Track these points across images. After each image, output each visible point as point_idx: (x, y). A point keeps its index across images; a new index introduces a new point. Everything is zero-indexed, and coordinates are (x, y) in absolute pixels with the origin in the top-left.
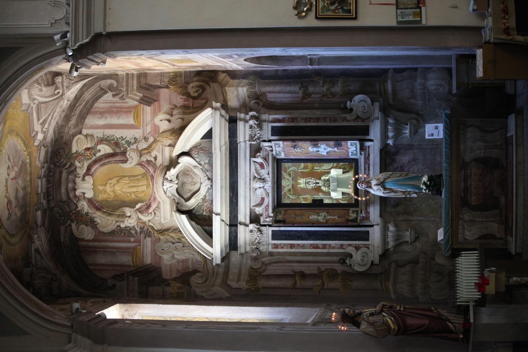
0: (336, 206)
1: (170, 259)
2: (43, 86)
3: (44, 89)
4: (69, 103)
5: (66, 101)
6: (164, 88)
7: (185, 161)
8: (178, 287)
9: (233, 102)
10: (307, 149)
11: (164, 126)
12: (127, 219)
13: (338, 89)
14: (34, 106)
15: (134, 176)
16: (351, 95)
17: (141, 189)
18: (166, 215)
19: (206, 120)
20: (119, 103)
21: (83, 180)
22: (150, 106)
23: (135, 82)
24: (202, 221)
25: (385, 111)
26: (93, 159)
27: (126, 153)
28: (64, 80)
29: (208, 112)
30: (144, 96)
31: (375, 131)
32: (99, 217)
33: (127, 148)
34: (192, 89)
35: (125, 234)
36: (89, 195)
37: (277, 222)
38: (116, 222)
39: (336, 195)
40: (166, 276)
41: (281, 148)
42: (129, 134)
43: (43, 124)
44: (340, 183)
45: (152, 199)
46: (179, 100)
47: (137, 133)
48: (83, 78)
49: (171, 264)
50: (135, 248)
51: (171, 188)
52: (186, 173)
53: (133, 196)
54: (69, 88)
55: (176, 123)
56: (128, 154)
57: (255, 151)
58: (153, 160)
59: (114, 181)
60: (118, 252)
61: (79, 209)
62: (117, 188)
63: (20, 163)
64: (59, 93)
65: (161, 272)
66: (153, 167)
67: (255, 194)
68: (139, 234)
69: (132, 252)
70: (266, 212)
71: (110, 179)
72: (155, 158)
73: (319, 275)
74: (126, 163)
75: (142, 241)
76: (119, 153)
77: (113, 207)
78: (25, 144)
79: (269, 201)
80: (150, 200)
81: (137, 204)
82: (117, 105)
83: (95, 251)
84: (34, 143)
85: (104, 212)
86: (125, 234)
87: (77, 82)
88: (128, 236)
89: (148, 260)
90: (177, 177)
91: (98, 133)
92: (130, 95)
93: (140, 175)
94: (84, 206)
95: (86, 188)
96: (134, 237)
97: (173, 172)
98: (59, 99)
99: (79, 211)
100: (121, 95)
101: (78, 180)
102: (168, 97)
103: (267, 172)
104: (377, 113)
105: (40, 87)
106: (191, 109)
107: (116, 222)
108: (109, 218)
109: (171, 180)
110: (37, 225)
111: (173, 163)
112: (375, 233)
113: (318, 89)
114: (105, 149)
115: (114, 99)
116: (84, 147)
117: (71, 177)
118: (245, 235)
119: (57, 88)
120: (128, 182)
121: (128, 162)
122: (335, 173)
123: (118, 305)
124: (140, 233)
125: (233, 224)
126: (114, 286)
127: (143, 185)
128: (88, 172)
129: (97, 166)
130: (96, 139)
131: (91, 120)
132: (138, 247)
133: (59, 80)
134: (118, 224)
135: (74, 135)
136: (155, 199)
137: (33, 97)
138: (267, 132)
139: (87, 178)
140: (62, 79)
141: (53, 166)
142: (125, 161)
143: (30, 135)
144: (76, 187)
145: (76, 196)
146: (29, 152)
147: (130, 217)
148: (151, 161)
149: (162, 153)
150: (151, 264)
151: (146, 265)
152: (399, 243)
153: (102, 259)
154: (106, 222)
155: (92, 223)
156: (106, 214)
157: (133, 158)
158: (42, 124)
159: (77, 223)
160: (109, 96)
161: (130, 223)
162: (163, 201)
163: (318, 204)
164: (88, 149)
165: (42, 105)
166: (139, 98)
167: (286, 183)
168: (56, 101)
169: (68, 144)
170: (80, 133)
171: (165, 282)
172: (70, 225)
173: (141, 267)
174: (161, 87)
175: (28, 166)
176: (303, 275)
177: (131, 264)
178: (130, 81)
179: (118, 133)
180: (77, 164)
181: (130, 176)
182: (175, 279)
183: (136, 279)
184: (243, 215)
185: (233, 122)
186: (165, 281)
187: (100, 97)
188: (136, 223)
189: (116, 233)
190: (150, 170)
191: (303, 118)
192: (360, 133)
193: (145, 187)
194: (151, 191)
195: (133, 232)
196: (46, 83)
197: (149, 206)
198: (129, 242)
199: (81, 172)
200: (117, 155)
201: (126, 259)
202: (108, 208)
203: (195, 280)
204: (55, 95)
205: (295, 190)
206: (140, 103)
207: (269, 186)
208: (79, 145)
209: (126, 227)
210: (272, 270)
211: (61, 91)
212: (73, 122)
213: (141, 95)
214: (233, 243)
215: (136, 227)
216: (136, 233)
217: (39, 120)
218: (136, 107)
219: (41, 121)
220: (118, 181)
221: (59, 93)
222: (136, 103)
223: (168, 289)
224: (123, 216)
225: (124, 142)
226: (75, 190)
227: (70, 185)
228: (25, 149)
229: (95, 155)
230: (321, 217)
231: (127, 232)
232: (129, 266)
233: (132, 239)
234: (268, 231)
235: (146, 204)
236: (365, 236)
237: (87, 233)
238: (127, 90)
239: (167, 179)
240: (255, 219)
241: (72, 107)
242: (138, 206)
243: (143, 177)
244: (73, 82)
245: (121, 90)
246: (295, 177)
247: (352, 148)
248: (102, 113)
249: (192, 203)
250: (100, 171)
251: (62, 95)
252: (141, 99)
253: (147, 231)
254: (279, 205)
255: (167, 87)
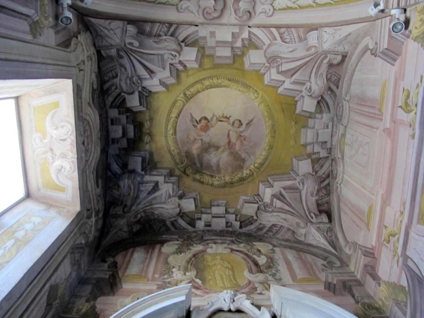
2: (317, 198)
3: (314, 199)
4: (302, 239)
5: (303, 231)
6: (355, 300)
8: (82, 309)
12: (183, 273)
14: (296, 182)
15: (235, 278)
20: (318, 268)
21: (226, 248)
22: (325, 288)
23: (348, 278)
26: (249, 254)
27: (261, 273)
28: (326, 225)
30: (335, 285)
33: (267, 273)
35: (164, 271)
36: (209, 251)
38: (179, 266)
40: (100, 300)
43: (280, 197)
45: (207, 291)
48: (331, 243)
49: (116, 304)
50: (146, 277)
53: (210, 278)
54: (318, 229)
56: (261, 274)
58: (259, 291)
59: (226, 264)
60: (144, 266)
61: (195, 245)
62: (218, 267)
63: (243, 156)
64: (312, 218)
65: (108, 295)
66: (249, 292)
68: (162, 280)
71: (229, 263)
72: (261, 294)
74: (250, 273)
75: (152, 282)
78: (262, 165)
80: (205, 289)
81: (200, 280)
82: (315, 267)
84: (262, 182)
85: (191, 259)
86: (164, 271)
87: (326, 239)
88: (161, 273)
89: (126, 286)
90: (239, 311)
92: (330, 275)
93: (237, 282)
96: (160, 277)
98: (306, 218)
99: (193, 245)
100: (325, 268)
101: (226, 245)
105: (315, 193)
107: (179, 266)
108: (184, 261)
109: (234, 301)
110: (181, 197)
115: (320, 265)
116: (260, 249)
117: (228, 242)
119: (316, 215)
120: (227, 273)
121: (251, 275)
123: (77, 208)
124: (163, 282)
126: (104, 261)
127: (224, 283)
129: (242, 255)
130: (271, 255)
131: (291, 255)
132: (146, 280)
133: (325, 218)
134: (177, 267)
135: (271, 244)
136: (207, 293)
137: (305, 181)
139: (229, 250)
140: (326, 223)
141: (237, 233)
142: (251, 271)
143: (269, 176)
144: (217, 244)
145: (208, 244)
146: (253, 174)
147: (185, 274)
148: (256, 290)
150: (122, 287)
151: (121, 284)
155: (179, 251)
156: (189, 260)
158: (281, 194)
159: (181, 244)
160: (320, 262)
162: (205, 299)
164: (259, 251)
165: (298, 194)
166: (330, 280)
168: (303, 215)
169: (260, 239)
170: (274, 246)
172: (178, 240)
173: (120, 280)
174: (353, 296)
175: (239, 175)
177: (126, 274)
178: (346, 275)
180: (242, 245)
181: (234, 275)
182: (94, 308)
183: (107, 277)
186: (95, 298)
187: (319, 257)
188: (176, 278)
189: (166, 265)
190: (244, 290)
193: (222, 285)
194: (218, 290)
195: (166, 276)
196: (320, 201)
197: (197, 288)
198: (154, 273)
199: (235, 247)
200: (257, 267)
202: (196, 261)
204: (310, 213)
206: (325, 283)
209: (172, 272)
211: (314, 220)
212: (283, 243)
213: (335, 282)
215: (172, 279)
216: (164, 279)
217: (285, 188)
218: (318, 279)
219: (283, 191)
220: (227, 267)
221: (312, 218)
222: (324, 279)
223: (83, 300)
224: (186, 270)
225: (274, 271)
226: (215, 243)
227: (219, 241)
228: (256, 165)
229: (253, 254)
232: (124, 273)
233: (157, 276)
235: (200, 287)
238: (334, 273)
239: (235, 295)
242: (197, 280)
243: (235, 284)
244: (325, 234)
245: (333, 269)
251: (311, 222)
252: (330, 283)
255: (357, 302)
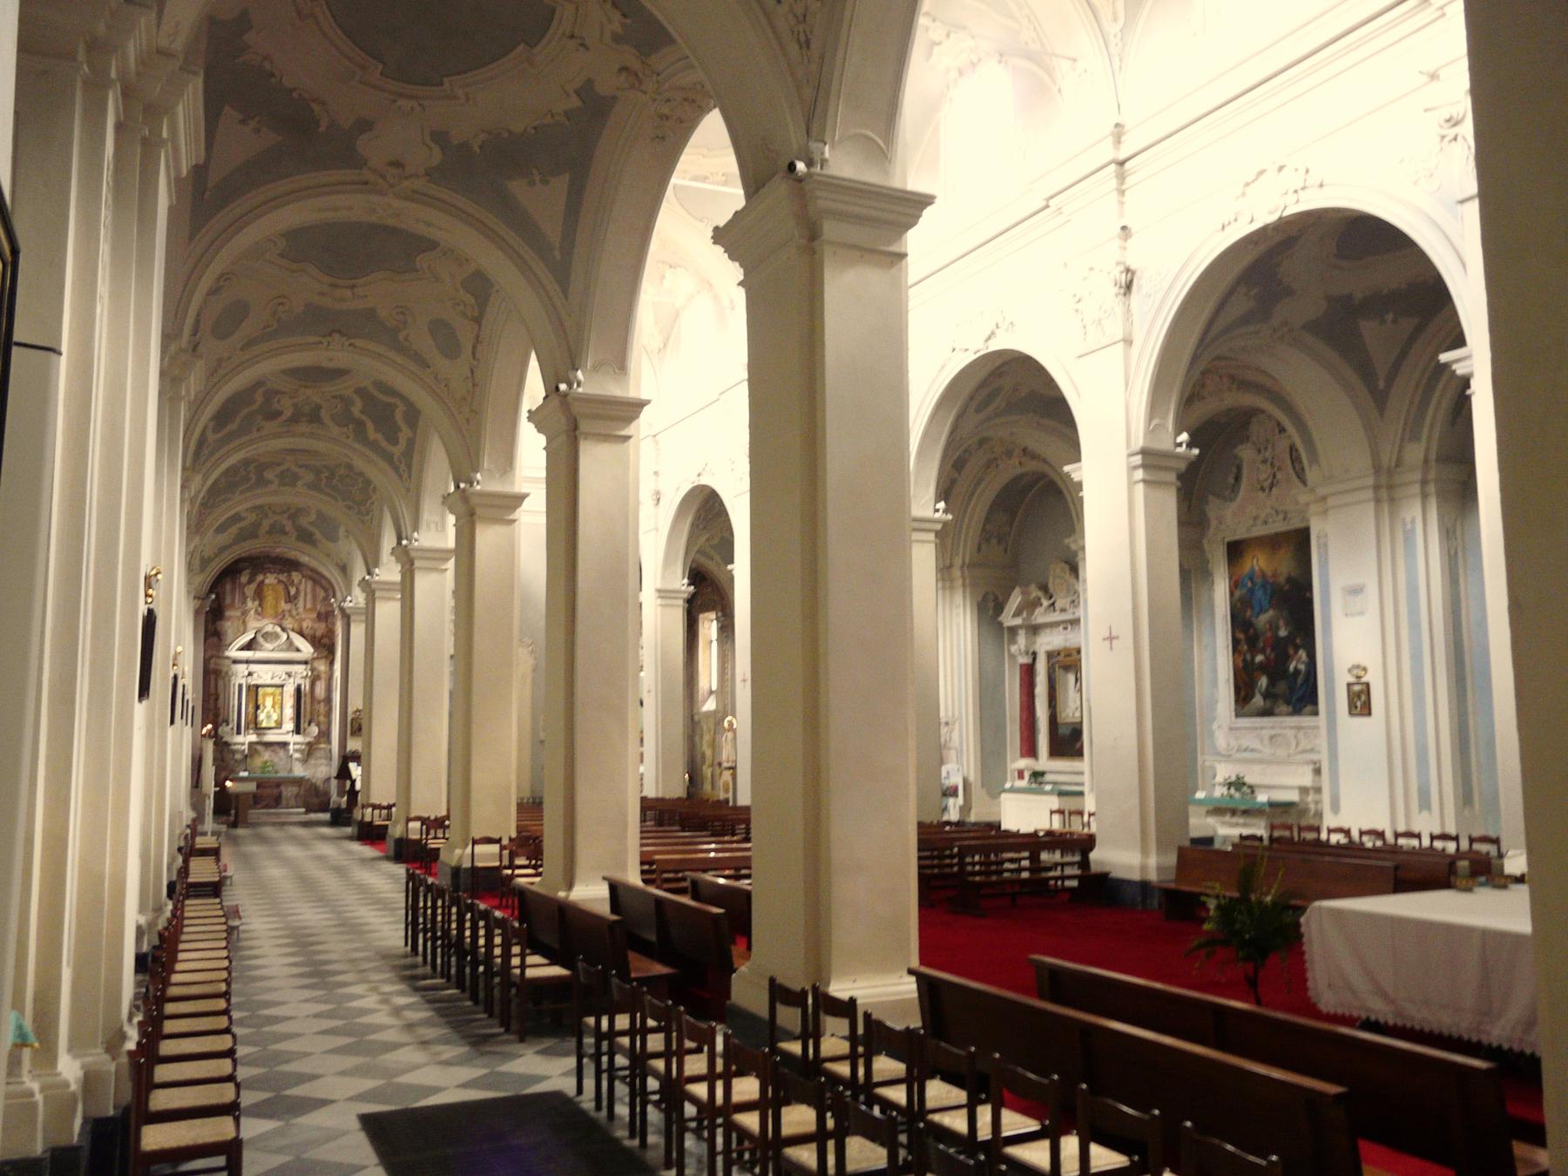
0: (256, 717)
1: (228, 626)
7: (284, 637)
9: (316, 664)
10: (289, 703)
11: (305, 625)
13: (322, 719)
16: (318, 725)
17: (270, 611)
18: (254, 624)
19: (307, 649)
24: (249, 646)
25: (309, 744)
29: (311, 650)
31: (299, 738)
32: (253, 586)
34: (325, 641)
37: (249, 687)
39: (262, 716)
41: (290, 690)
42: (301, 604)
44: (269, 717)
46: (319, 634)
47: (301, 610)
51: (269, 628)
52: (277, 636)
55: (306, 632)
57: (289, 675)
67: (264, 674)
69: (232, 605)
70: (254, 681)
73: (216, 708)
76: (290, 599)
77: (259, 595)
79: (259, 682)
83: (234, 583)
89: (228, 613)
91: (302, 588)
94: (260, 578)
95: (270, 579)
97: (278, 629)
102: (321, 628)
103: (277, 681)
104: (308, 739)
106: (314, 641)
111: (283, 630)
112: (240, 739)
113: (322, 708)
114: (293, 591)
118: (242, 669)
122: (275, 717)
125: (248, 662)
128: (280, 581)
131: (310, 584)
138: (299, 681)
149: (289, 623)
152: (234, 752)
153: (228, 587)
154: (250, 590)
155: (250, 582)
157: (287, 607)
161: (250, 604)
163: (257, 707)
167: (270, 690)
171: (214, 622)
176: (217, 699)
179: (301, 598)
184: (253, 667)
185: (306, 663)
191: (306, 700)
192: (297, 730)
201: (228, 601)
203: (215, 639)
205: (265, 695)
207: (269, 682)
208: (296, 576)
210: (220, 683)
214: (235, 662)
230: (251, 709)
231: (244, 602)
234: (243, 681)
236: (239, 733)
237: (244, 579)
240: (250, 674)
241: (317, 573)
246: (273, 695)
247: (289, 725)
248: (314, 591)
249: (260, 639)
250: (281, 588)
253: (245, 613)
254: (257, 687)
